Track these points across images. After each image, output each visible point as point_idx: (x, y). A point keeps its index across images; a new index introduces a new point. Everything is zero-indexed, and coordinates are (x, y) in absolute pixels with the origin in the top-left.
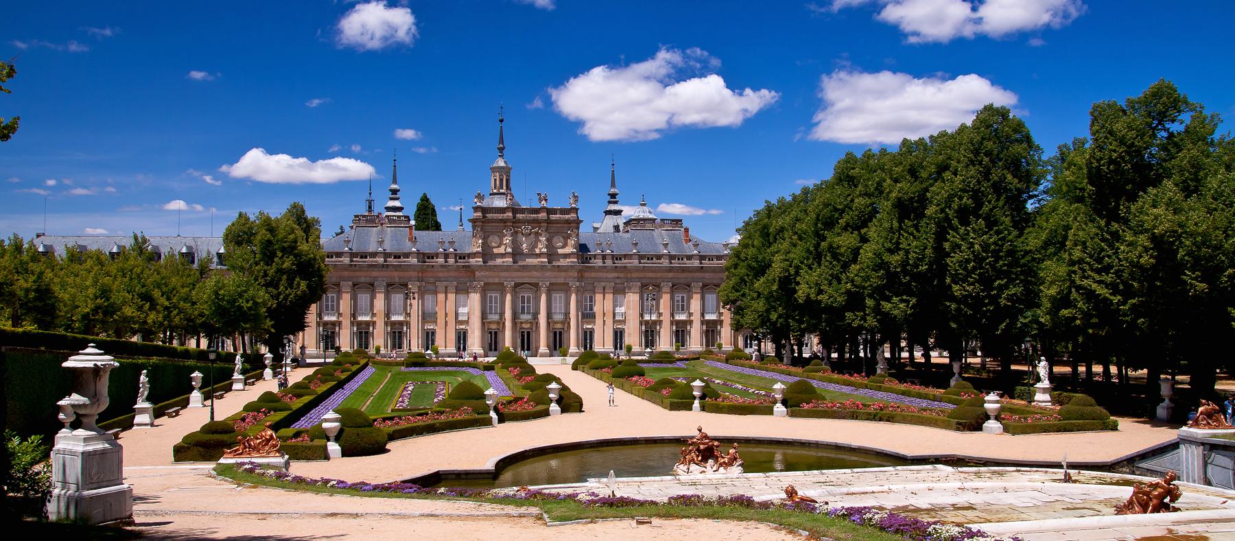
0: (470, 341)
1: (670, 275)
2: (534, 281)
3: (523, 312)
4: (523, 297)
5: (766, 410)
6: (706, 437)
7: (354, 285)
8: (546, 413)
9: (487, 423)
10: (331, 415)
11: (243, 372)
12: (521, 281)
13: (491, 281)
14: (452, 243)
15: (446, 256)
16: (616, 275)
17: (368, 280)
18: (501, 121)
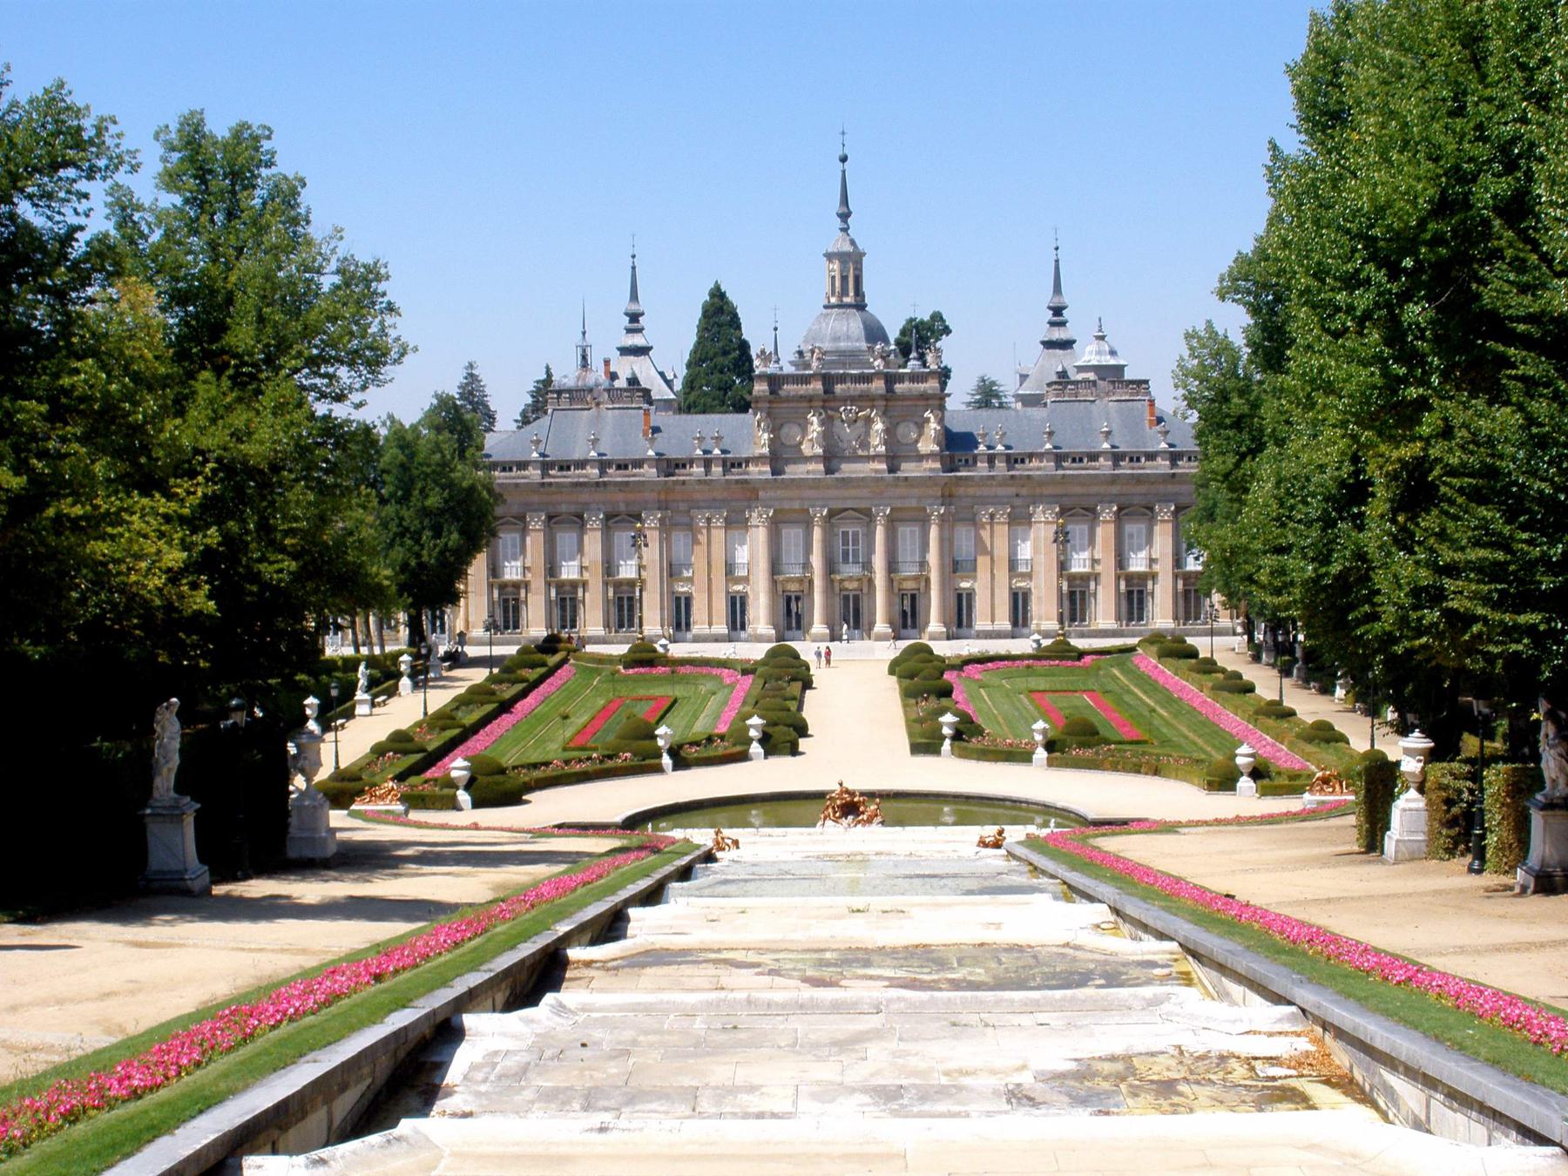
0: (751, 613)
1: (1115, 490)
2: (863, 505)
3: (846, 560)
4: (845, 534)
6: (847, 792)
7: (550, 518)
8: (743, 757)
9: (659, 769)
10: (460, 762)
11: (368, 689)
12: (839, 505)
13: (786, 505)
14: (719, 439)
15: (707, 464)
16: (1013, 490)
17: (573, 509)
18: (844, 159)
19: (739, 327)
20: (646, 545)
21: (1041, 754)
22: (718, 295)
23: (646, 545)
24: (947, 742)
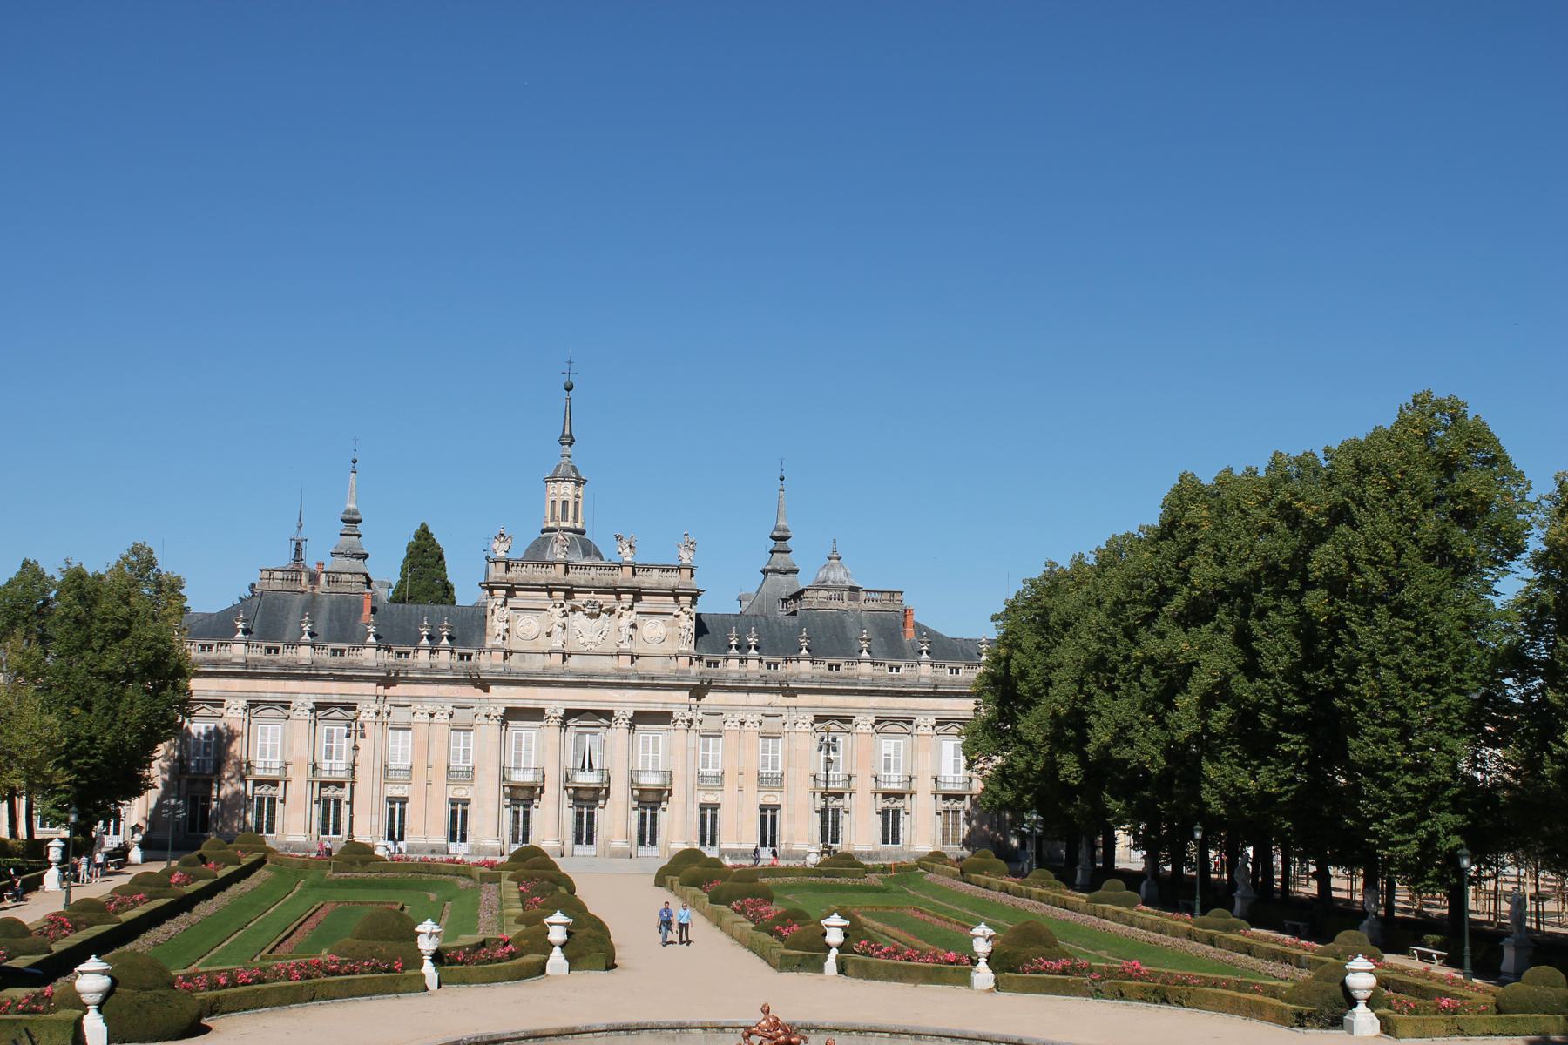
5: (955, 971)
6: (776, 1024)
18: (569, 388)
19: (443, 568)
20: (363, 736)
21: (983, 975)
22: (424, 534)
23: (363, 736)
24: (834, 952)
